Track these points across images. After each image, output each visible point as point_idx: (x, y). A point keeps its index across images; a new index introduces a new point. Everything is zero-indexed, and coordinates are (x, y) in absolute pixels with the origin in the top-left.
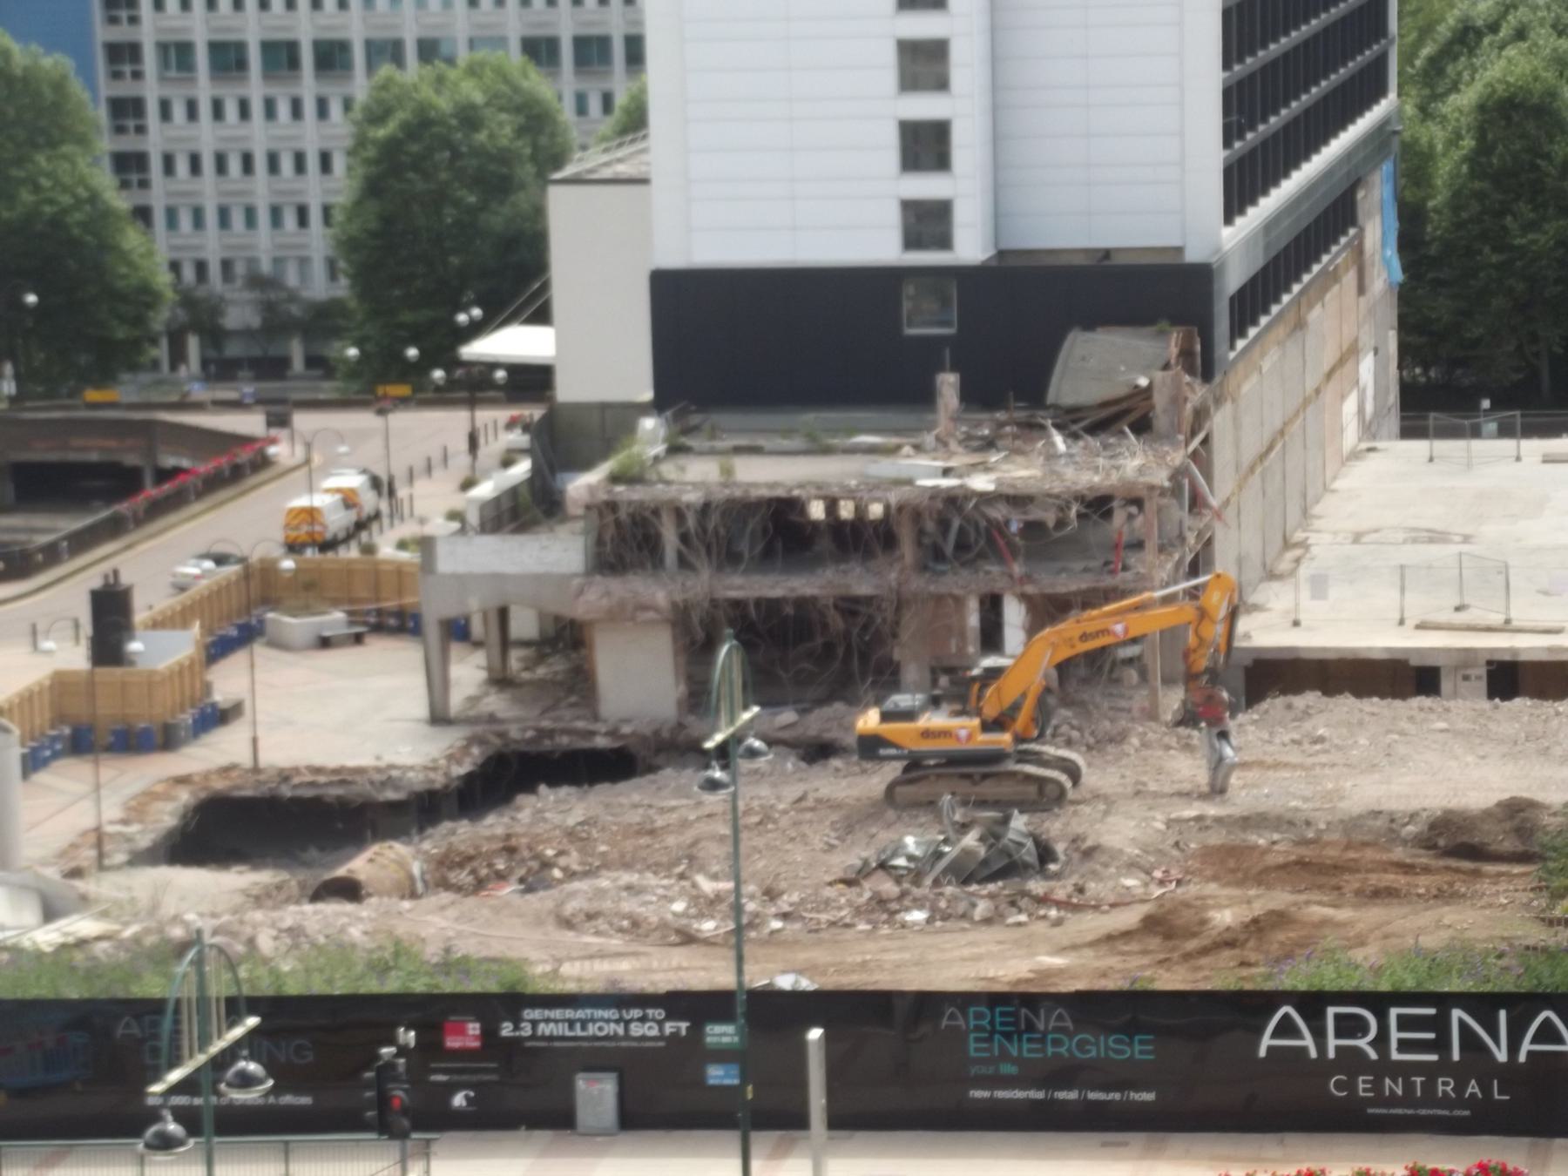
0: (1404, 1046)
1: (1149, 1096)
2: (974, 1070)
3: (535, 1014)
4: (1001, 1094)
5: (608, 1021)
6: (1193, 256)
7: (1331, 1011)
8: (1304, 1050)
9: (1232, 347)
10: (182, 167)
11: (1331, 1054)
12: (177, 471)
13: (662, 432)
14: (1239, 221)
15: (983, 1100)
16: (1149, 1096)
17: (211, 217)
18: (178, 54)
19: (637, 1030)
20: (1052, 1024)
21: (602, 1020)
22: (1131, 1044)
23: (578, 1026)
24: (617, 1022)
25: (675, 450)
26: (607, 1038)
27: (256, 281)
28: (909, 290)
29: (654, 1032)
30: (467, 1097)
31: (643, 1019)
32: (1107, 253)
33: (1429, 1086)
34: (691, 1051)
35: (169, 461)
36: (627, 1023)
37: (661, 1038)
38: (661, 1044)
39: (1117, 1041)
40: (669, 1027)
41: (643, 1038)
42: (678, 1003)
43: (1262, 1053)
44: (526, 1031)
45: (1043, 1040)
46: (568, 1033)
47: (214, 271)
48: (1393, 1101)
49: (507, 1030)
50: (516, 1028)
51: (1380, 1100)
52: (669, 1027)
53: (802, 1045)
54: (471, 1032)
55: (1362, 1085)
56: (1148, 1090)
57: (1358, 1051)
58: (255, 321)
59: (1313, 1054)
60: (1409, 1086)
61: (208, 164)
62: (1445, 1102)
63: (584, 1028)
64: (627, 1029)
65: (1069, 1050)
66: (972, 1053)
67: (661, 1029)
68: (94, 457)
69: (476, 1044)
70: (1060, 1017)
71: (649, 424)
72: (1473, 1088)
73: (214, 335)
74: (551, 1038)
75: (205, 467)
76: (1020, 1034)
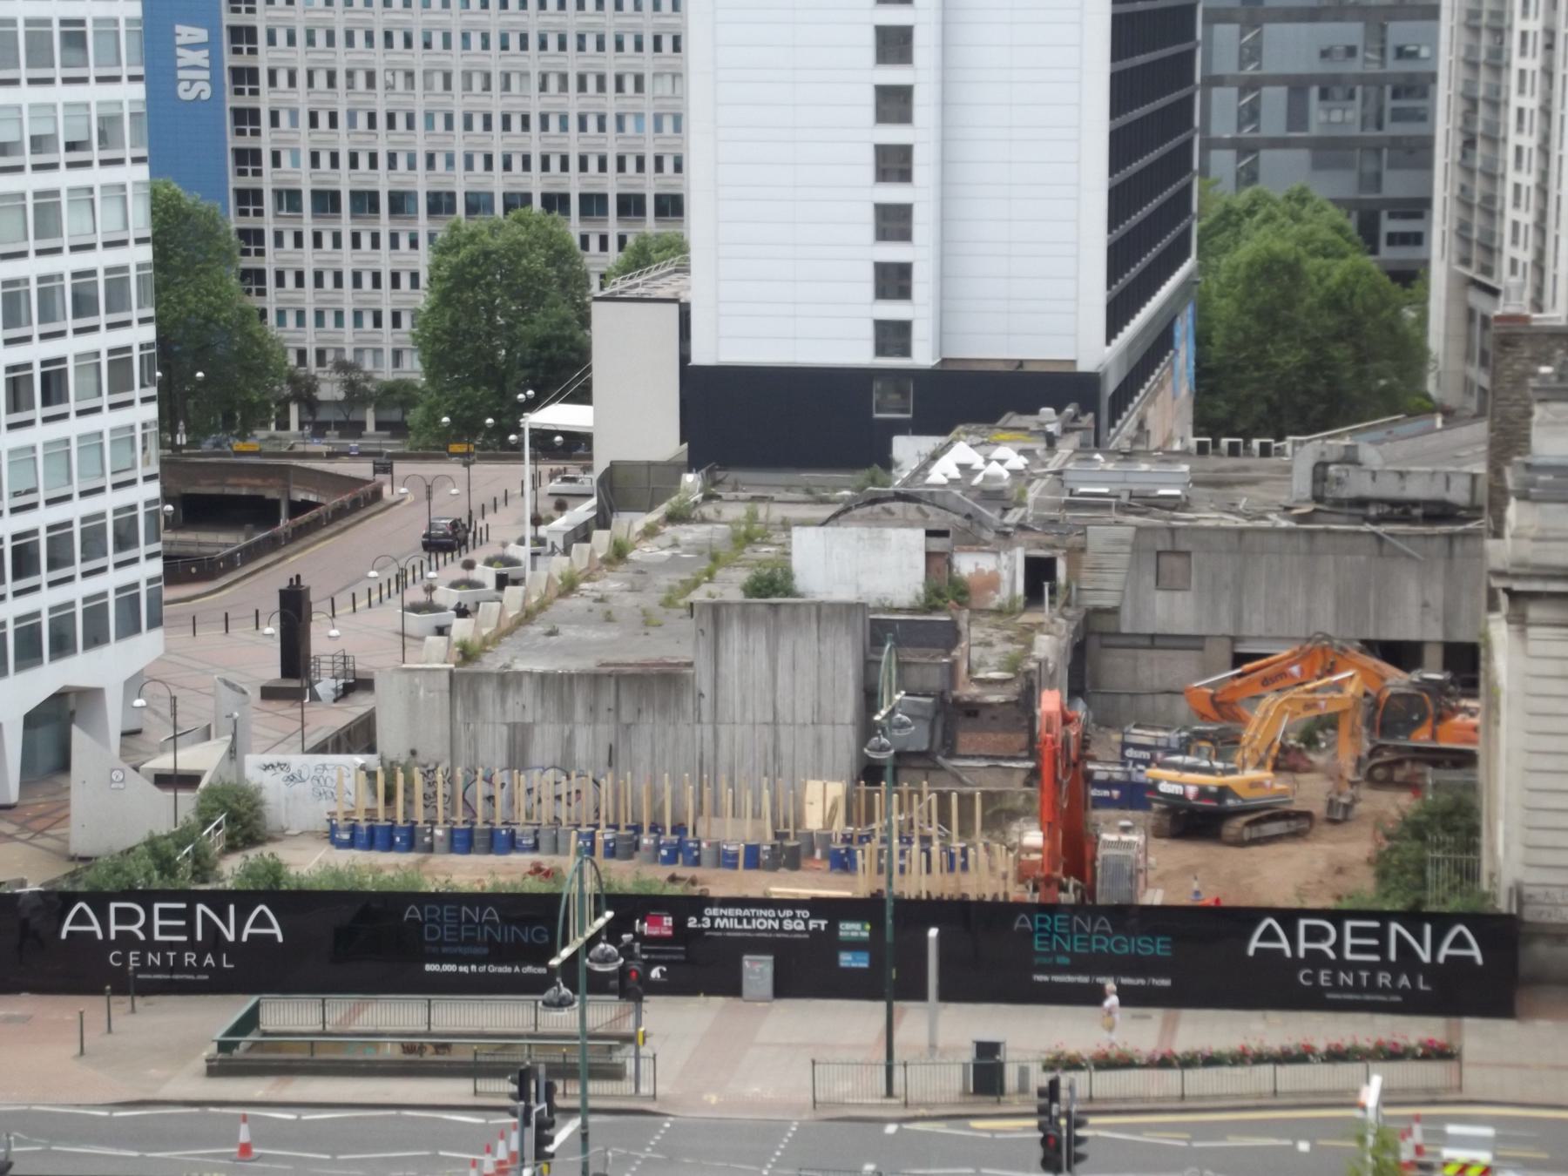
0: (1356, 949)
1: (1166, 982)
2: (1037, 960)
3: (715, 911)
4: (1057, 978)
5: (767, 918)
7: (1303, 923)
8: (1281, 951)
10: (290, 280)
11: (1302, 954)
12: (313, 505)
13: (699, 484)
14: (1115, 343)
15: (1043, 983)
16: (1166, 982)
18: (289, 199)
19: (788, 925)
20: (1096, 928)
21: (763, 917)
22: (1154, 945)
23: (745, 921)
24: (774, 919)
25: (708, 498)
26: (766, 930)
27: (342, 366)
28: (877, 386)
29: (802, 927)
30: (661, 971)
31: (793, 918)
32: (1021, 363)
33: (1372, 979)
34: (829, 943)
35: (300, 496)
36: (781, 920)
37: (807, 931)
38: (806, 936)
39: (1144, 942)
40: (812, 924)
41: (793, 931)
42: (817, 906)
43: (1251, 952)
44: (707, 924)
45: (1089, 941)
46: (737, 926)
47: (311, 357)
48: (1346, 989)
49: (692, 923)
50: (699, 921)
51: (1336, 987)
52: (812, 924)
53: (924, 939)
55: (1324, 978)
56: (1165, 977)
57: (1321, 953)
58: (341, 395)
59: (1288, 953)
60: (1357, 979)
62: (1384, 990)
63: (749, 922)
64: (781, 924)
65: (1108, 948)
66: (1037, 948)
68: (244, 492)
69: (669, 933)
70: (1103, 924)
71: (689, 478)
72: (1404, 981)
73: (310, 404)
74: (725, 929)
75: (332, 502)
76: (1072, 934)
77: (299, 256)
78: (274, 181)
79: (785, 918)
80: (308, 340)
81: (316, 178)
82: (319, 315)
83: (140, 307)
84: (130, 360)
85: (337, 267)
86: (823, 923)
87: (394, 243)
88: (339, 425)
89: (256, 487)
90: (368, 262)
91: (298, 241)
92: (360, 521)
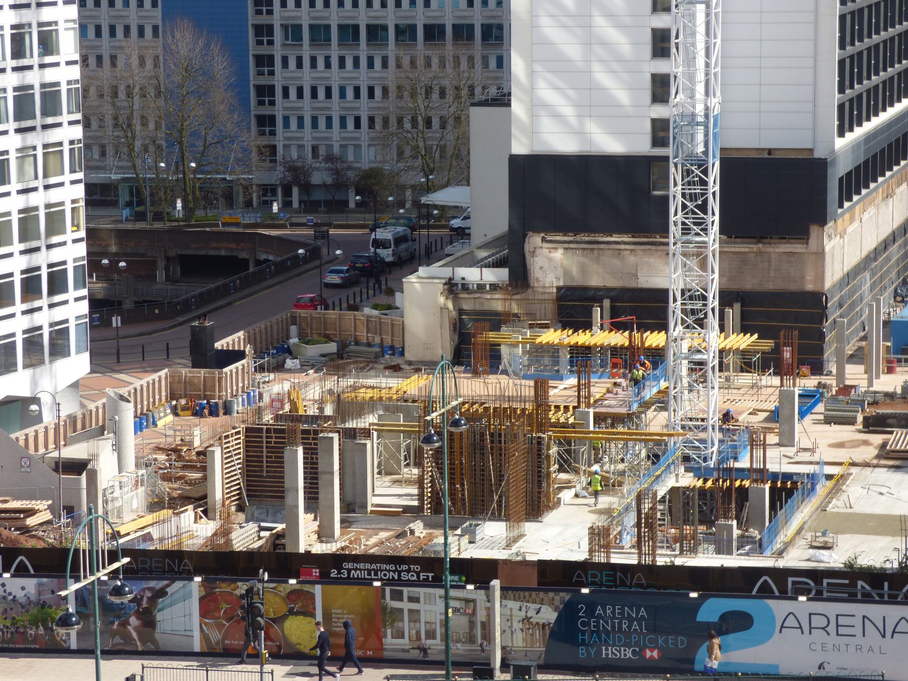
3: (350, 565)
5: (389, 571)
6: (818, 154)
7: (790, 580)
9: (841, 206)
10: (293, 93)
17: (308, 122)
18: (293, 32)
21: (386, 570)
23: (373, 572)
24: (394, 572)
29: (415, 578)
31: (408, 571)
35: (263, 257)
46: (366, 577)
50: (339, 573)
54: (314, 574)
58: (329, 181)
61: (307, 92)
64: (399, 576)
67: (418, 577)
68: (223, 253)
73: (306, 188)
77: (300, 75)
78: (282, 18)
79: (402, 571)
80: (306, 139)
81: (312, 15)
82: (315, 120)
83: (69, 112)
84: (61, 152)
85: (327, 83)
86: (431, 575)
87: (371, 65)
88: (327, 203)
89: (231, 250)
90: (350, 79)
91: (300, 65)
92: (299, 275)
